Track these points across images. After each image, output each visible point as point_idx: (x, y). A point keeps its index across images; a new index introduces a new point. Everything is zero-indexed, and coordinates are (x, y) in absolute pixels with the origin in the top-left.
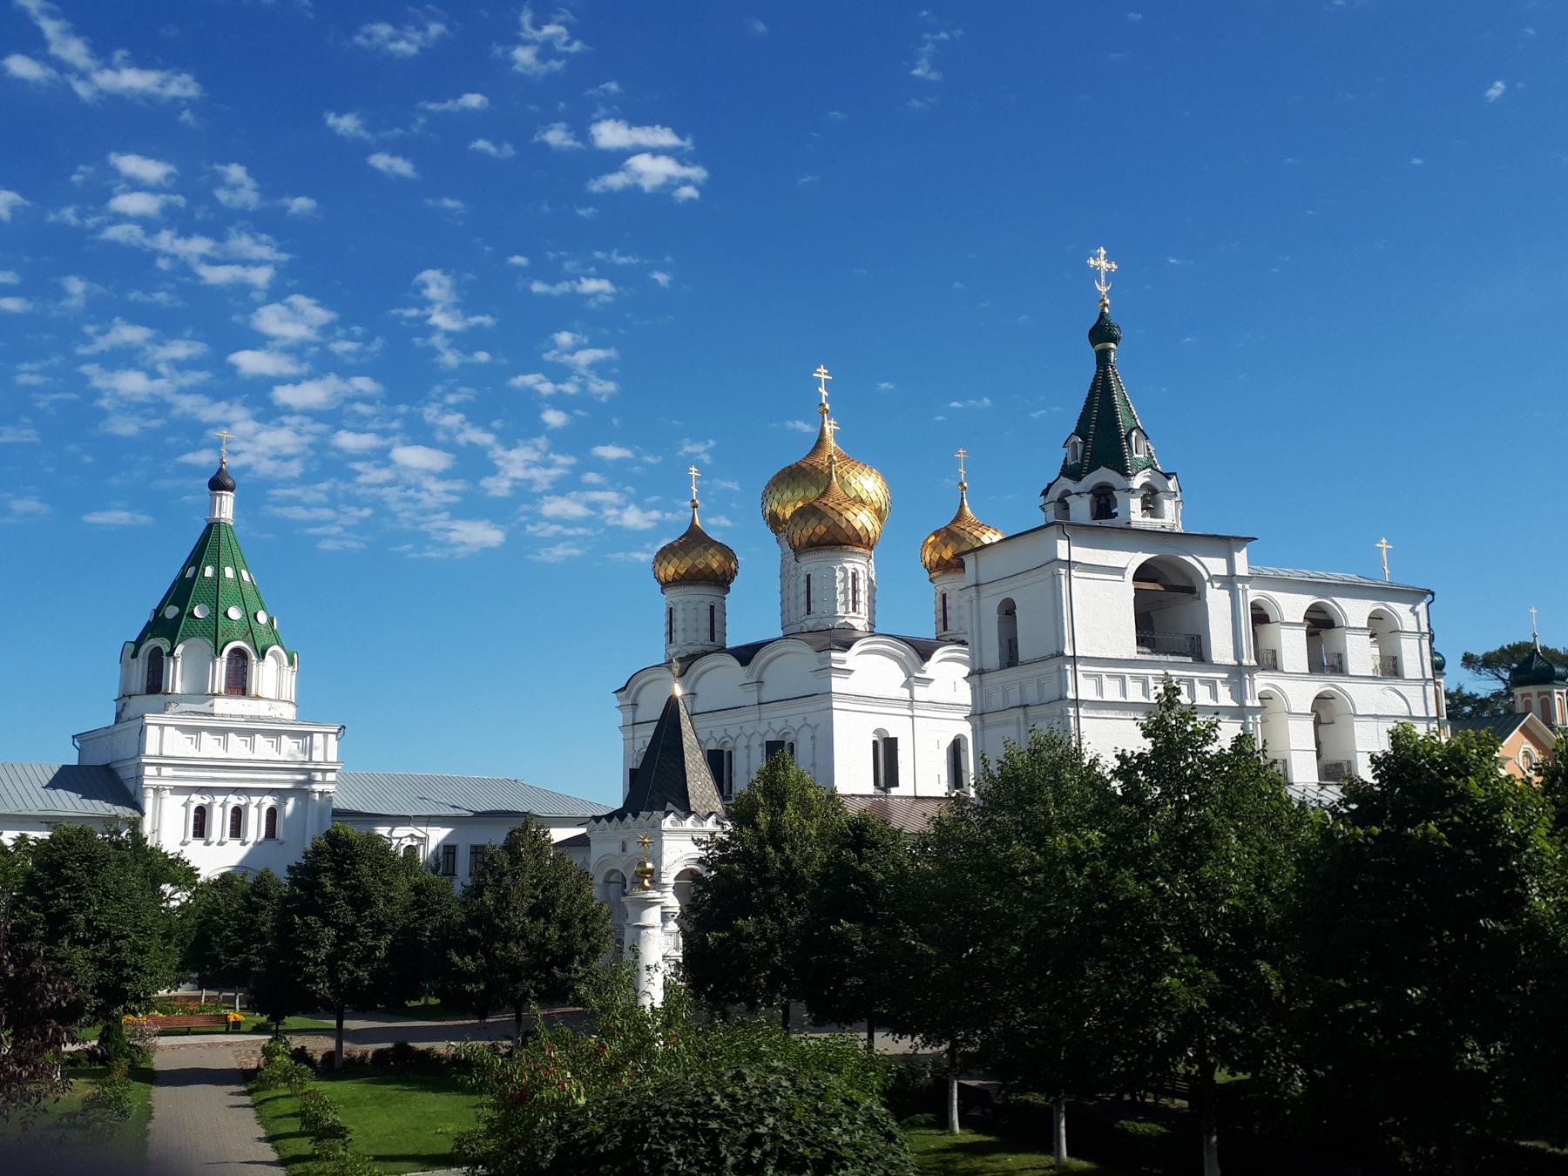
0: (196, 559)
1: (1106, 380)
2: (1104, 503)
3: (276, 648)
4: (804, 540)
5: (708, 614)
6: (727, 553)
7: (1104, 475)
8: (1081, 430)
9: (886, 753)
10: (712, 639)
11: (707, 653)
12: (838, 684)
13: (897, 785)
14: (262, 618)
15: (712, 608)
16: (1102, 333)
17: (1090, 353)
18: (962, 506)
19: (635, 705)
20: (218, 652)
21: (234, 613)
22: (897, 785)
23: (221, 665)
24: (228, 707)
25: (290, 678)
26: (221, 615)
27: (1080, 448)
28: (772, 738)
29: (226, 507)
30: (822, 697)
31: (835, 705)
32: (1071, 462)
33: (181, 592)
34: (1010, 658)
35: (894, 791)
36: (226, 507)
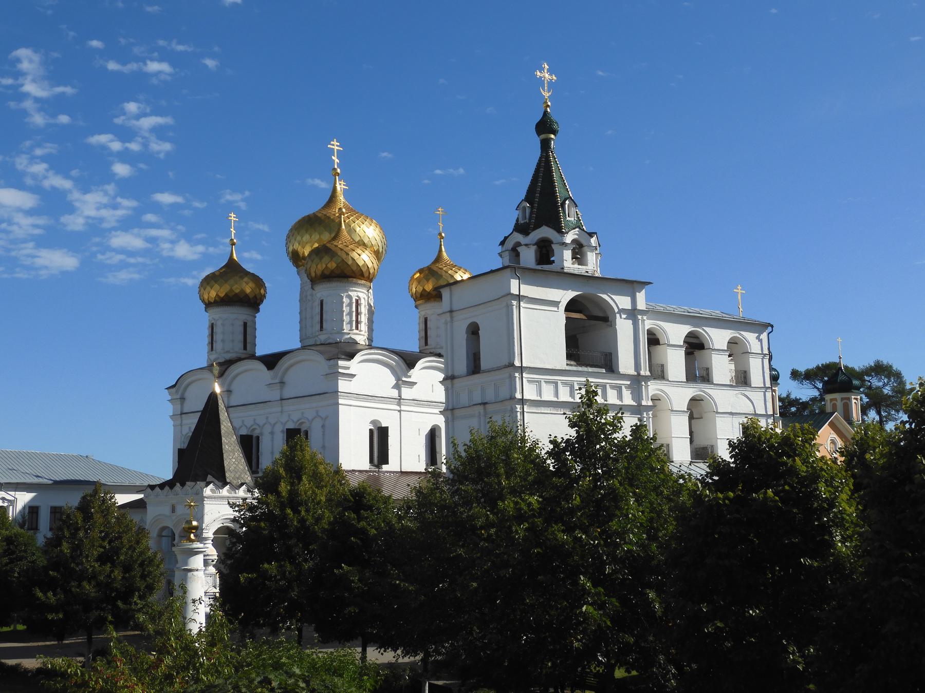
1: (548, 162)
2: (545, 252)
4: (319, 273)
5: (242, 329)
6: (258, 282)
7: (545, 232)
8: (529, 197)
9: (380, 439)
10: (245, 348)
11: (240, 359)
12: (343, 385)
13: (387, 463)
15: (245, 325)
16: (545, 126)
17: (536, 141)
18: (440, 251)
22: (387, 463)
27: (528, 211)
28: (291, 426)
30: (329, 396)
31: (341, 401)
32: (521, 221)
34: (475, 367)
35: (385, 468)
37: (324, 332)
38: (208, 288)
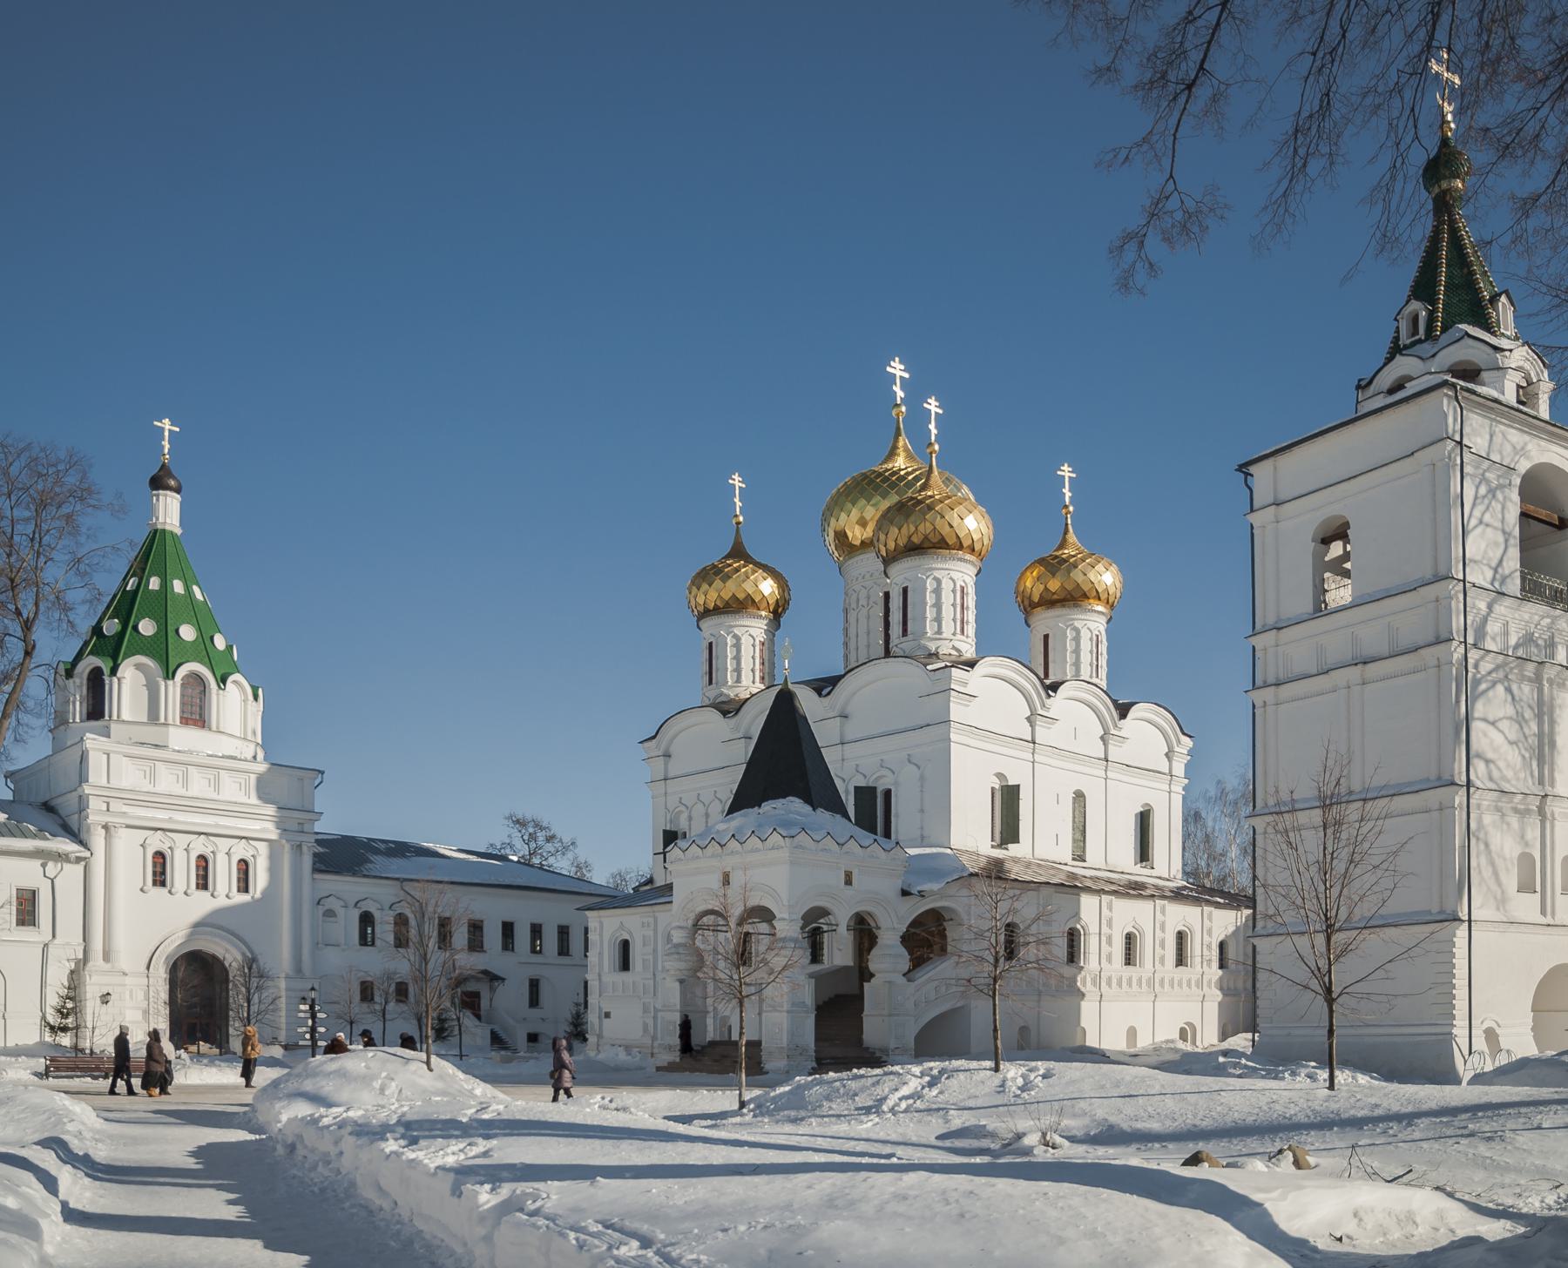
0: (140, 567)
3: (237, 677)
4: (901, 543)
9: (1008, 799)
13: (1016, 840)
14: (220, 642)
19: (667, 755)
20: (169, 674)
21: (188, 633)
22: (1016, 840)
23: (172, 692)
24: (182, 738)
25: (256, 710)
26: (171, 634)
29: (169, 511)
33: (125, 606)
36: (169, 511)
37: (910, 637)
38: (705, 586)
